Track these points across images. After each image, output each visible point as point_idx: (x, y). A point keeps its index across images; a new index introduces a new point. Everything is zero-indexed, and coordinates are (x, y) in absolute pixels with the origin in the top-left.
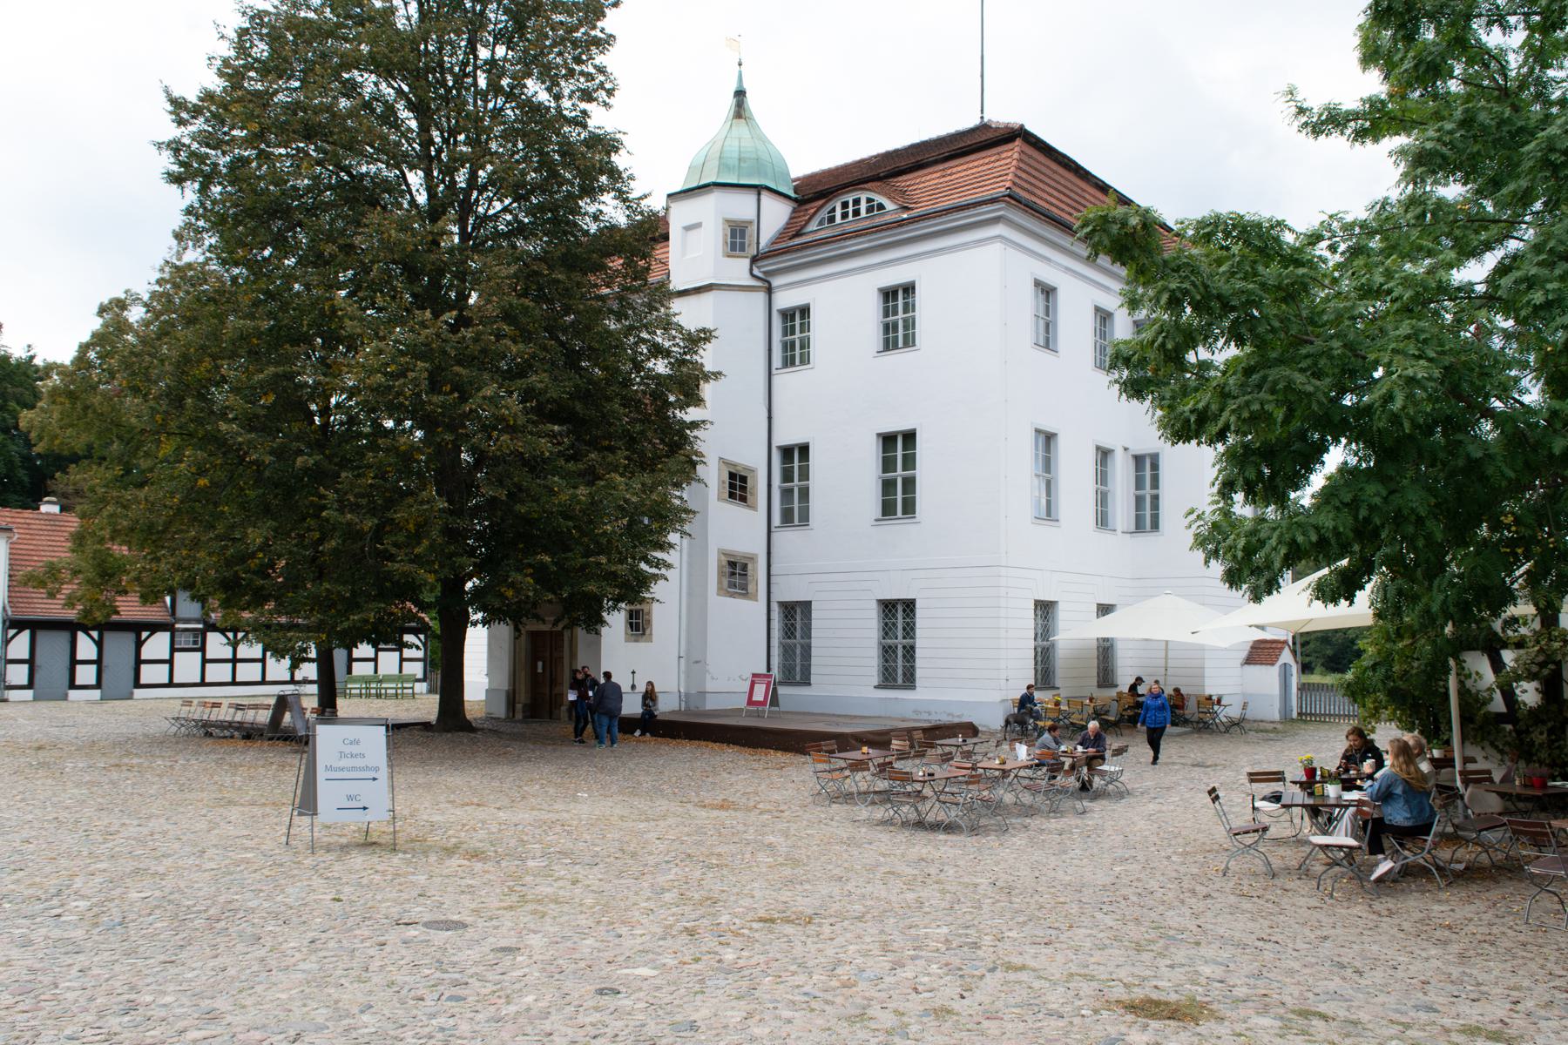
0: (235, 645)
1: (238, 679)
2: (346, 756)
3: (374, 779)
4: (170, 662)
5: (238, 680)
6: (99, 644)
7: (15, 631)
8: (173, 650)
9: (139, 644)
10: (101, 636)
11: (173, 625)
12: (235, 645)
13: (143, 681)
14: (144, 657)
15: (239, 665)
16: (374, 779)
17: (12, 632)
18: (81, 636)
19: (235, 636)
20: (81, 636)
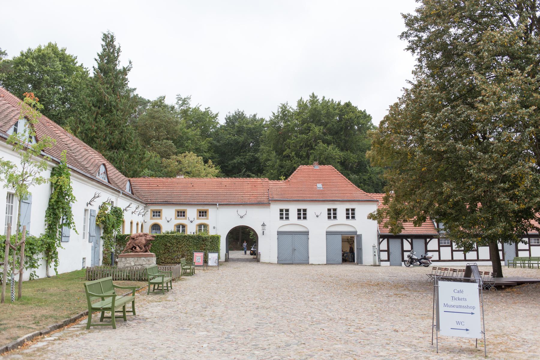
2: (455, 299)
3: (472, 313)
4: (439, 251)
6: (411, 244)
7: (382, 239)
8: (439, 246)
9: (426, 244)
10: (412, 241)
14: (428, 249)
16: (472, 313)
17: (381, 240)
18: (405, 240)
20: (405, 240)
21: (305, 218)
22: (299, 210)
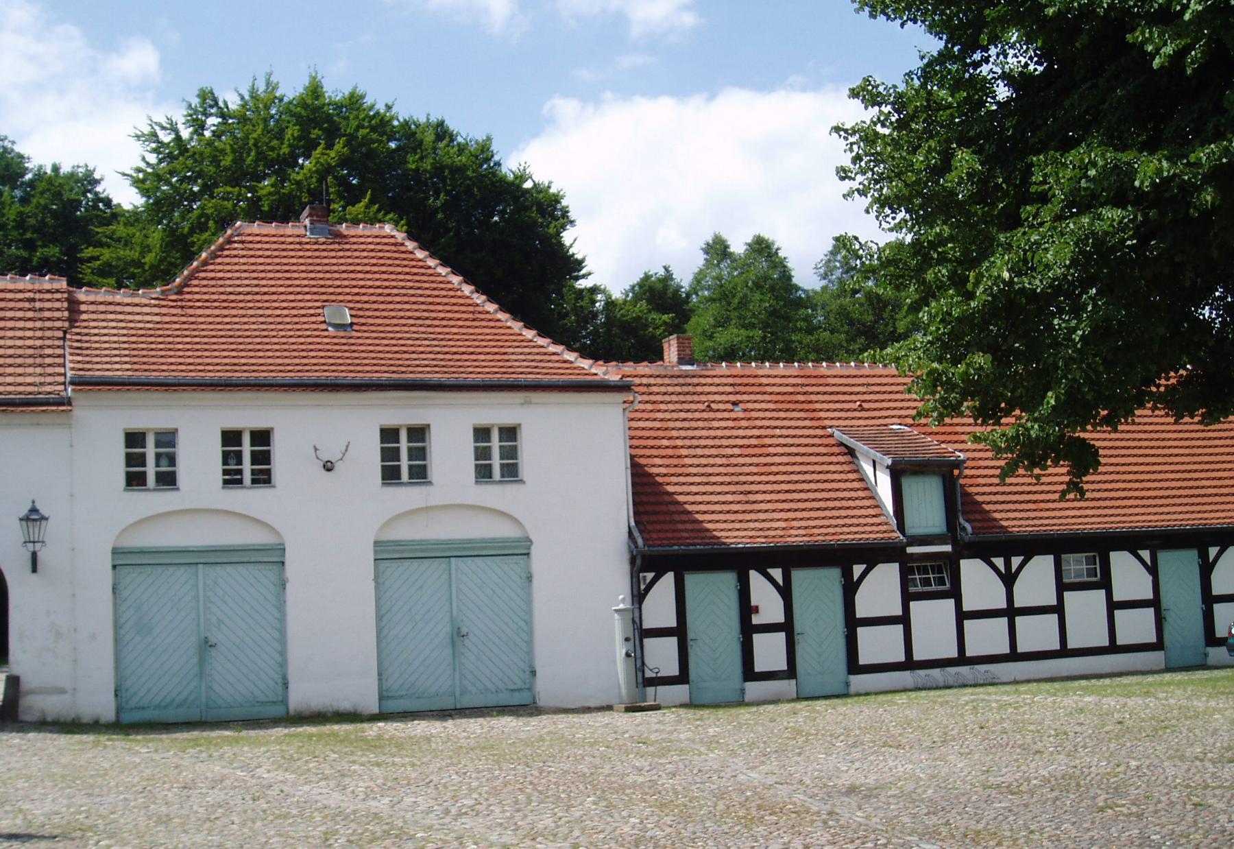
0: (1009, 579)
1: (1021, 649)
5: (1021, 649)
6: (785, 591)
8: (907, 598)
9: (850, 589)
11: (902, 548)
12: (1009, 579)
13: (863, 660)
14: (860, 613)
15: (1019, 620)
18: (755, 577)
19: (1008, 564)
20: (755, 577)
21: (263, 478)
22: (231, 438)
